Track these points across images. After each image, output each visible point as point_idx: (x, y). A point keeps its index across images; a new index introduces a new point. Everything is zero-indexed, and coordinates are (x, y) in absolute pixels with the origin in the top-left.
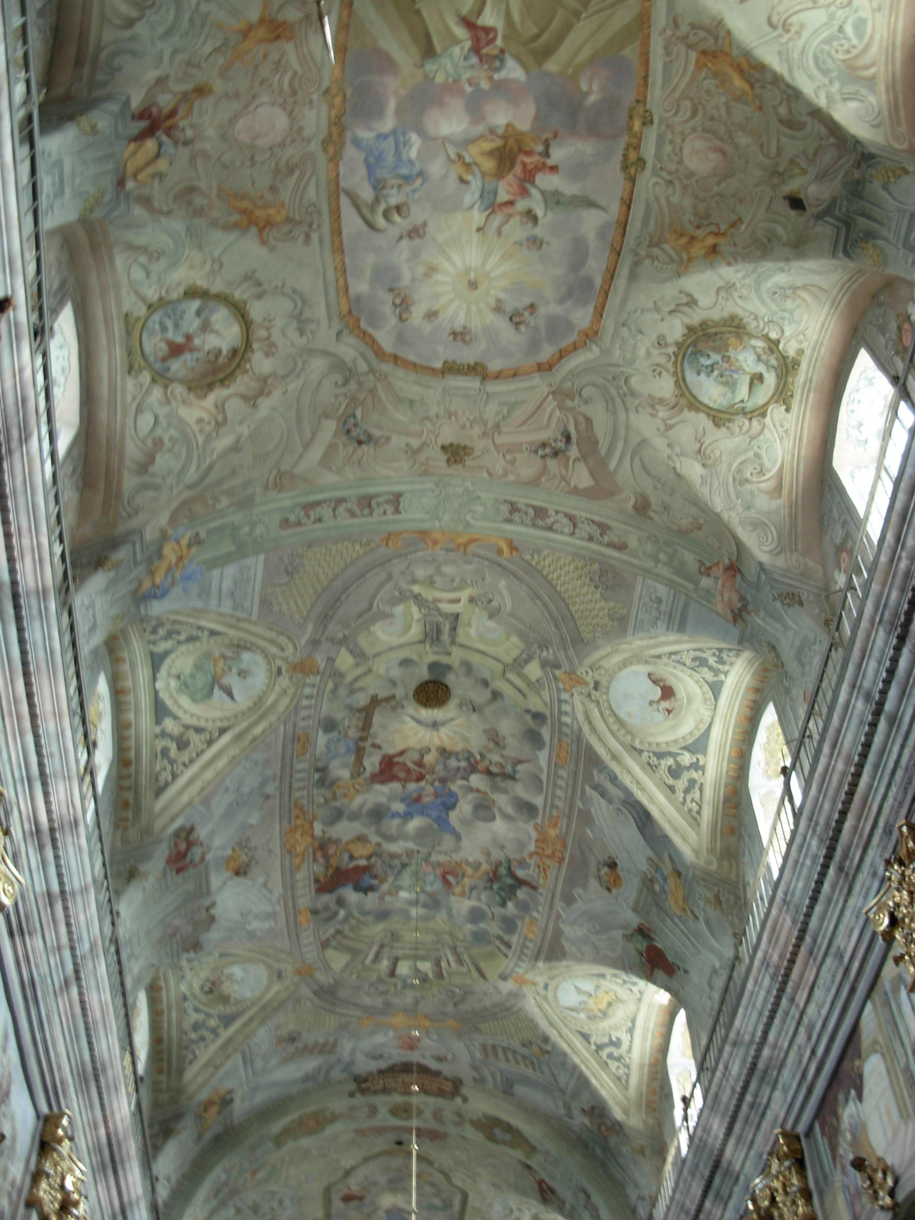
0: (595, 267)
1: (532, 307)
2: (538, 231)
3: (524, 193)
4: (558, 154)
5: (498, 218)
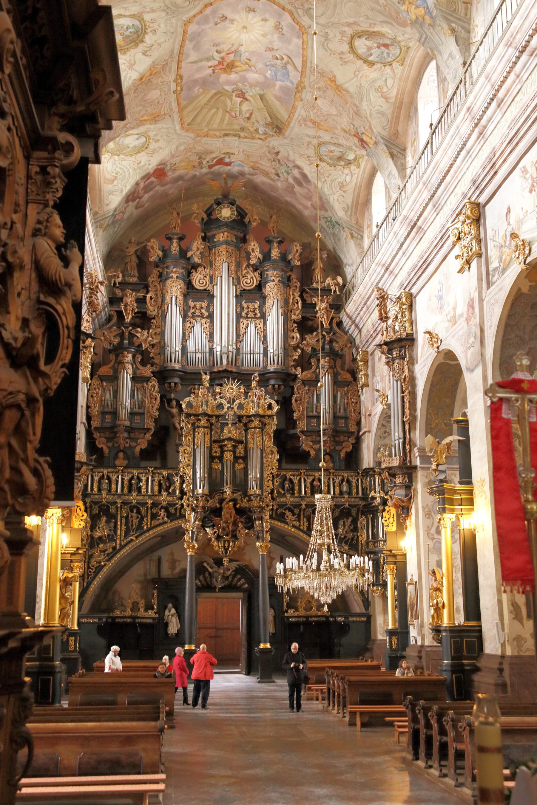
0: (189, 45)
1: (216, 24)
2: (216, 48)
3: (223, 58)
4: (210, 71)
5: (233, 49)
